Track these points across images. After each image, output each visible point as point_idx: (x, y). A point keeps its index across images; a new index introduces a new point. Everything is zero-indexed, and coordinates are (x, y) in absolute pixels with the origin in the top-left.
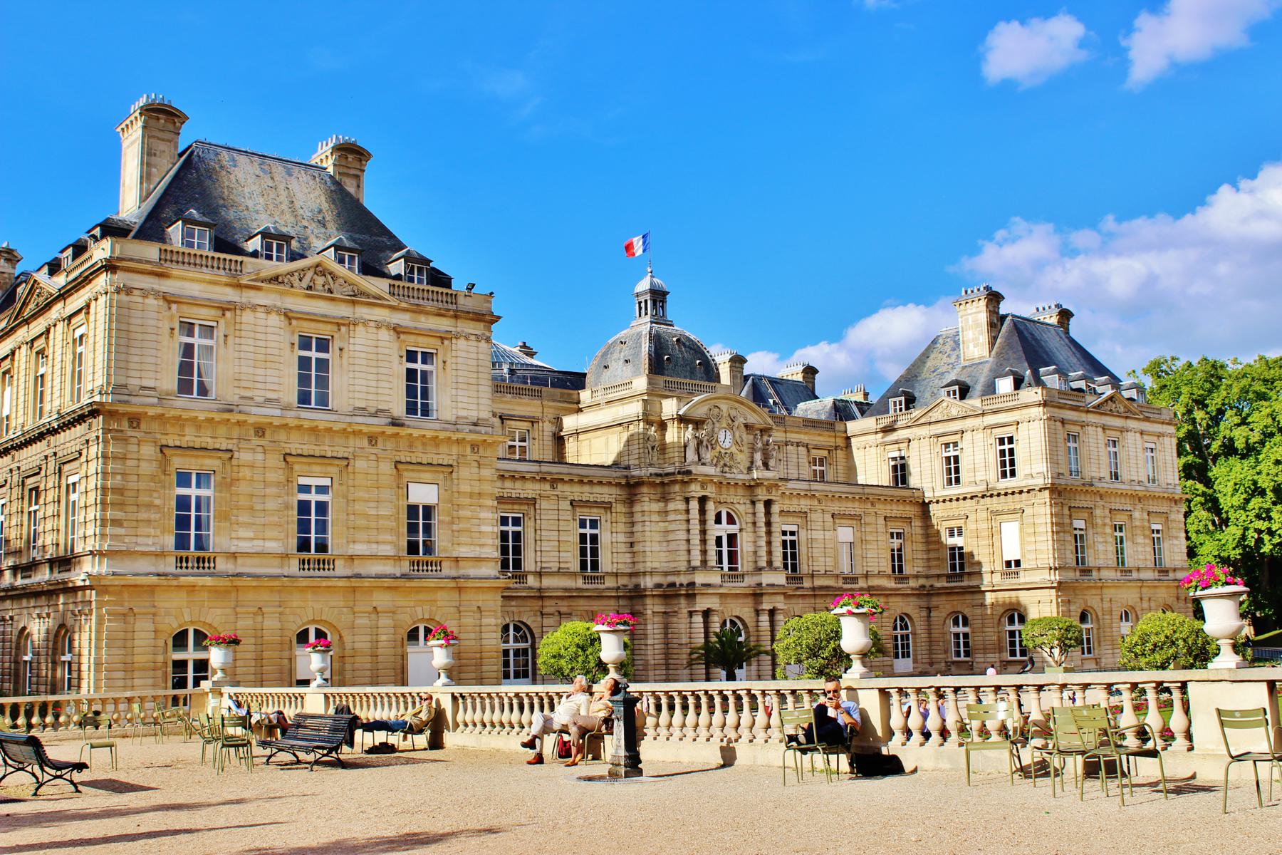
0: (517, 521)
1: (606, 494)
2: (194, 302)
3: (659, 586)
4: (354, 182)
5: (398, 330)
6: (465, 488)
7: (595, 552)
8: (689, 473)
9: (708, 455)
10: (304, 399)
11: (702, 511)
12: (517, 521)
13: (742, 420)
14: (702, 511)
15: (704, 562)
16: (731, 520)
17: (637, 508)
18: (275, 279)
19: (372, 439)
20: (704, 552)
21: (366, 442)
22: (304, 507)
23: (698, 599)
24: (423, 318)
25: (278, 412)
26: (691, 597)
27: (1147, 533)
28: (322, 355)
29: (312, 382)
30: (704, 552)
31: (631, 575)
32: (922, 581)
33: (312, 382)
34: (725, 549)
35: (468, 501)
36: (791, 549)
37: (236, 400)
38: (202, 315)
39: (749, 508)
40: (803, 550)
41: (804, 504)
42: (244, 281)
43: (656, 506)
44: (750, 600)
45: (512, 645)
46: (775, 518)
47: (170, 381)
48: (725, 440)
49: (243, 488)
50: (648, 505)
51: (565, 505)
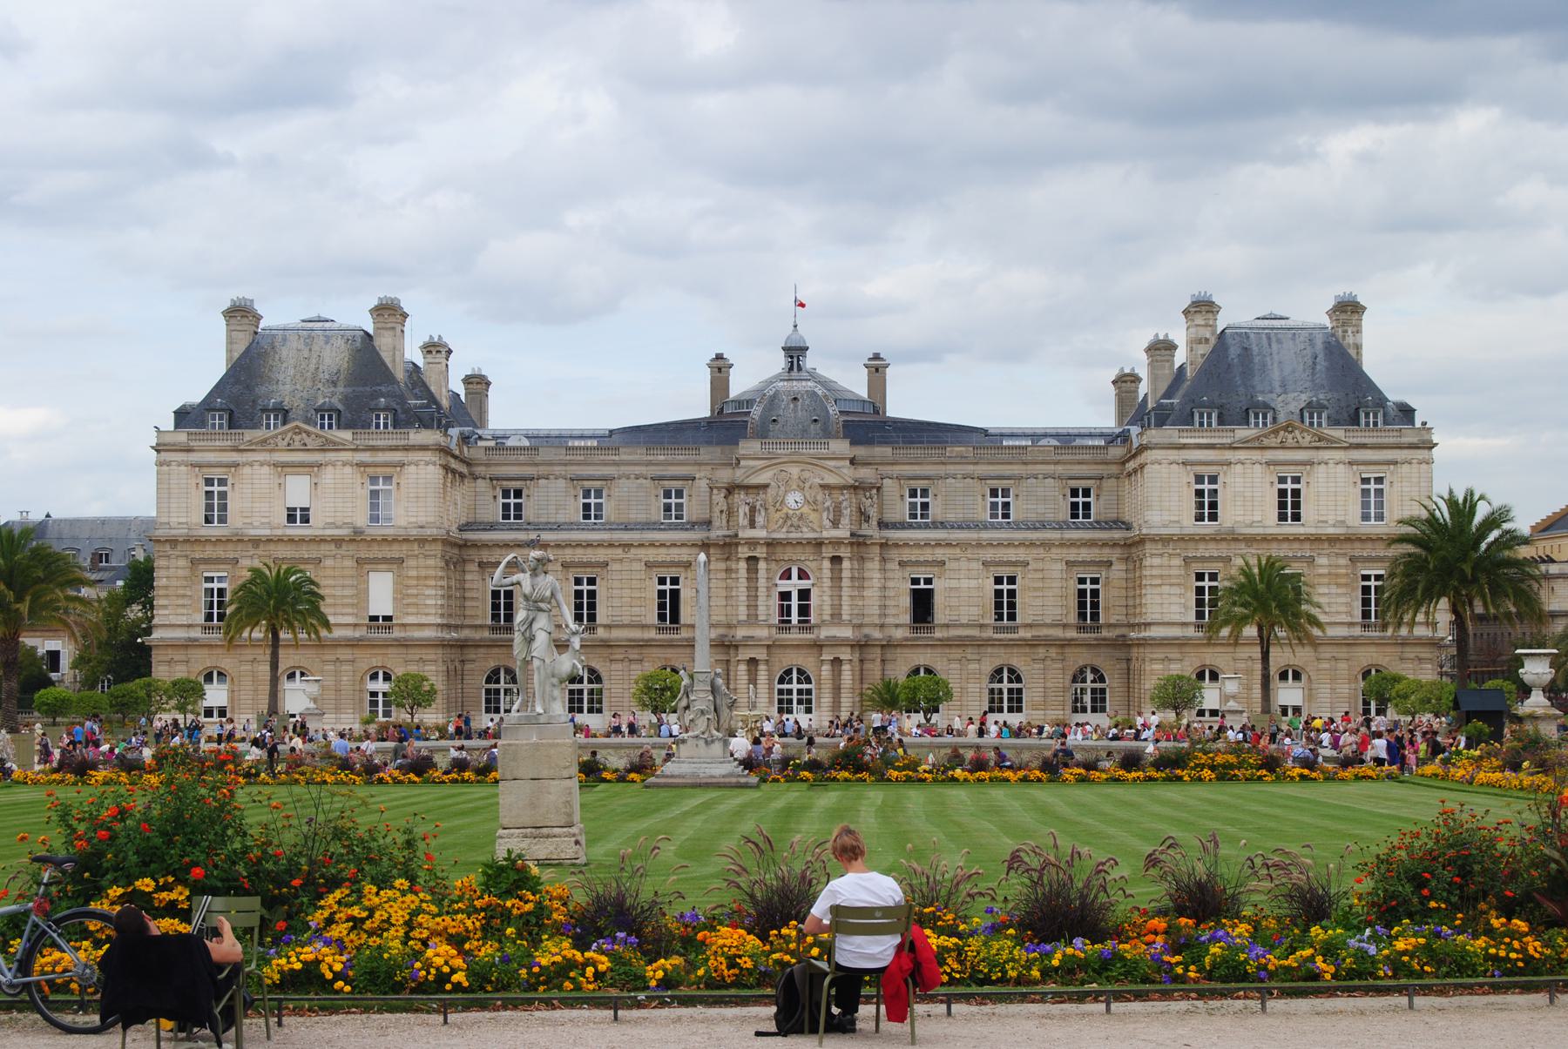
1: (683, 554)
2: (210, 465)
4: (391, 333)
6: (413, 573)
9: (760, 519)
12: (592, 581)
13: (818, 481)
15: (752, 620)
16: (803, 575)
18: (265, 441)
20: (752, 606)
21: (333, 546)
23: (741, 650)
25: (268, 532)
26: (736, 647)
30: (752, 606)
32: (1118, 632)
34: (795, 603)
37: (239, 525)
38: (216, 473)
40: (938, 600)
43: (722, 565)
44: (815, 650)
48: (793, 499)
51: (640, 566)
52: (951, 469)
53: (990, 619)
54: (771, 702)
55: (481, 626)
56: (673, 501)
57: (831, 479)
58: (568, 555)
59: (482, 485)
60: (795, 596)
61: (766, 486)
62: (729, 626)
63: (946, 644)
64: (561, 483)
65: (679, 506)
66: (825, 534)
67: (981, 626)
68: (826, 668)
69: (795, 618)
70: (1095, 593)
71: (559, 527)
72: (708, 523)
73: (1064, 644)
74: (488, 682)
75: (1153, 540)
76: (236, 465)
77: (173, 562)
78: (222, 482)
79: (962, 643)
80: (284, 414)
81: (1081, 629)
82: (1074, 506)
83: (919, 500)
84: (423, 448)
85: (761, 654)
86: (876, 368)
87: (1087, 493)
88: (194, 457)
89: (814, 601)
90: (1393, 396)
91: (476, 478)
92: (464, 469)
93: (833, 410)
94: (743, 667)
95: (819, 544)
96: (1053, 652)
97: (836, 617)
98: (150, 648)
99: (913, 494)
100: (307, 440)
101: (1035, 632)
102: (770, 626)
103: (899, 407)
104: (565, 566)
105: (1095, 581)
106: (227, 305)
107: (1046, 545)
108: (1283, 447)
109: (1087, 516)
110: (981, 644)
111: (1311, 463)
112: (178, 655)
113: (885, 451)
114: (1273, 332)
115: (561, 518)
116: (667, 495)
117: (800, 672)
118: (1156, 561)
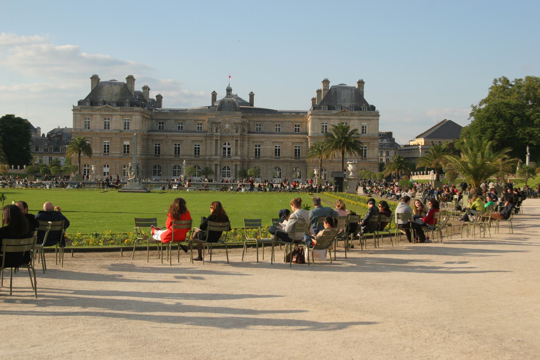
0: (179, 145)
1: (201, 139)
2: (86, 114)
3: (210, 159)
5: (122, 115)
7: (199, 151)
9: (219, 131)
10: (105, 128)
11: (217, 143)
12: (179, 145)
14: (217, 143)
15: (216, 155)
16: (229, 144)
18: (99, 110)
19: (116, 134)
20: (216, 151)
22: (105, 146)
29: (107, 126)
30: (216, 151)
33: (107, 126)
34: (227, 151)
38: (87, 117)
41: (262, 140)
43: (210, 141)
47: (83, 127)
48: (227, 126)
50: (208, 141)
52: (266, 119)
53: (274, 156)
54: (221, 174)
55: (152, 155)
57: (236, 121)
58: (173, 138)
59: (154, 121)
60: (227, 149)
61: (220, 123)
62: (211, 156)
64: (173, 121)
65: (201, 127)
67: (272, 157)
68: (234, 167)
69: (227, 154)
70: (299, 150)
71: (171, 131)
72: (207, 132)
73: (292, 162)
74: (154, 168)
76: (92, 115)
78: (89, 119)
79: (267, 161)
80: (104, 103)
81: (295, 158)
82: (296, 129)
83: (258, 127)
84: (137, 112)
85: (218, 163)
86: (252, 96)
87: (299, 126)
88: (82, 113)
89: (231, 151)
90: (370, 103)
91: (152, 119)
92: (150, 117)
93: (237, 104)
94: (214, 166)
95: (233, 137)
96: (289, 164)
97: (236, 155)
99: (257, 125)
101: (285, 159)
102: (221, 156)
103: (256, 105)
104: (173, 141)
105: (299, 147)
106: (91, 76)
107: (288, 138)
108: (343, 115)
109: (298, 131)
110: (272, 161)
111: (350, 119)
113: (251, 115)
114: (342, 88)
115: (173, 129)
116: (198, 124)
117: (228, 167)
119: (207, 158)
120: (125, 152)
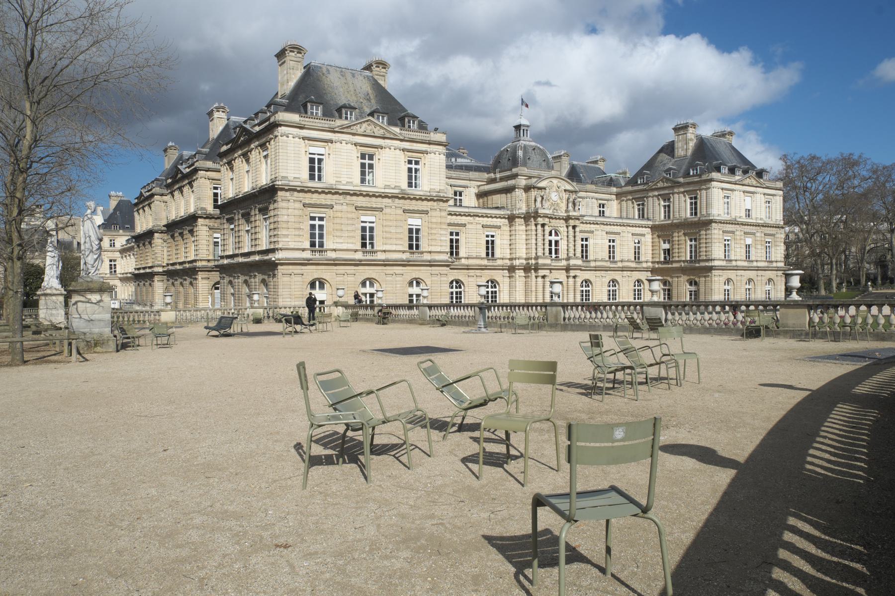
6: (434, 220)
8: (536, 212)
9: (546, 205)
16: (556, 234)
17: (513, 228)
24: (415, 144)
27: (763, 243)
28: (371, 162)
31: (511, 259)
34: (553, 248)
35: (434, 226)
36: (585, 249)
37: (334, 183)
39: (565, 229)
42: (336, 129)
45: (454, 290)
46: (577, 234)
47: (305, 174)
48: (554, 197)
49: (338, 221)
56: (458, 197)
57: (569, 187)
61: (545, 189)
63: (596, 269)
66: (571, 214)
68: (571, 280)
69: (554, 256)
75: (716, 222)
77: (291, 205)
88: (305, 133)
98: (277, 265)
100: (375, 130)
112: (297, 269)
118: (716, 231)
119: (517, 263)
120: (411, 247)
